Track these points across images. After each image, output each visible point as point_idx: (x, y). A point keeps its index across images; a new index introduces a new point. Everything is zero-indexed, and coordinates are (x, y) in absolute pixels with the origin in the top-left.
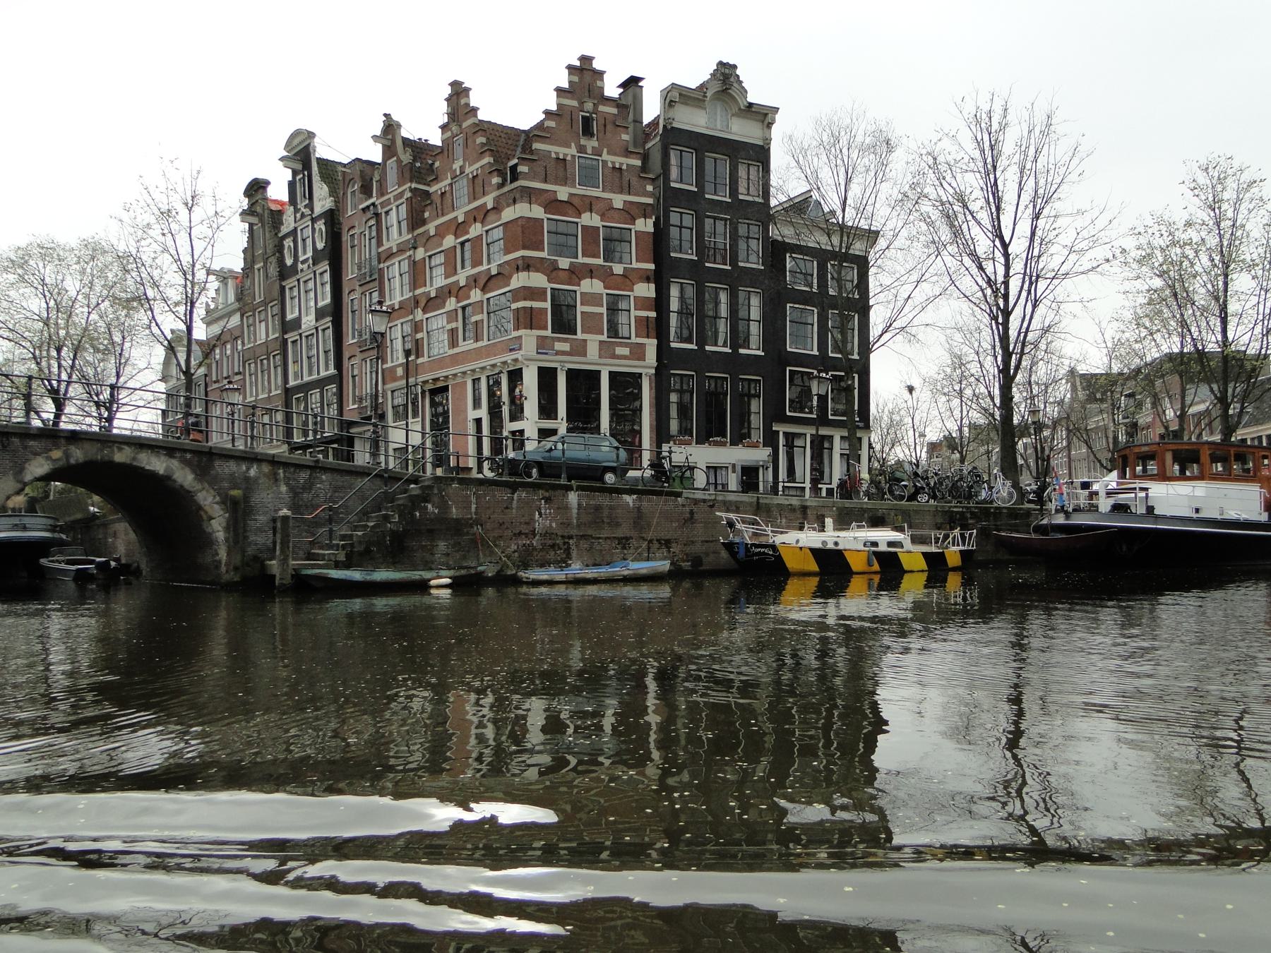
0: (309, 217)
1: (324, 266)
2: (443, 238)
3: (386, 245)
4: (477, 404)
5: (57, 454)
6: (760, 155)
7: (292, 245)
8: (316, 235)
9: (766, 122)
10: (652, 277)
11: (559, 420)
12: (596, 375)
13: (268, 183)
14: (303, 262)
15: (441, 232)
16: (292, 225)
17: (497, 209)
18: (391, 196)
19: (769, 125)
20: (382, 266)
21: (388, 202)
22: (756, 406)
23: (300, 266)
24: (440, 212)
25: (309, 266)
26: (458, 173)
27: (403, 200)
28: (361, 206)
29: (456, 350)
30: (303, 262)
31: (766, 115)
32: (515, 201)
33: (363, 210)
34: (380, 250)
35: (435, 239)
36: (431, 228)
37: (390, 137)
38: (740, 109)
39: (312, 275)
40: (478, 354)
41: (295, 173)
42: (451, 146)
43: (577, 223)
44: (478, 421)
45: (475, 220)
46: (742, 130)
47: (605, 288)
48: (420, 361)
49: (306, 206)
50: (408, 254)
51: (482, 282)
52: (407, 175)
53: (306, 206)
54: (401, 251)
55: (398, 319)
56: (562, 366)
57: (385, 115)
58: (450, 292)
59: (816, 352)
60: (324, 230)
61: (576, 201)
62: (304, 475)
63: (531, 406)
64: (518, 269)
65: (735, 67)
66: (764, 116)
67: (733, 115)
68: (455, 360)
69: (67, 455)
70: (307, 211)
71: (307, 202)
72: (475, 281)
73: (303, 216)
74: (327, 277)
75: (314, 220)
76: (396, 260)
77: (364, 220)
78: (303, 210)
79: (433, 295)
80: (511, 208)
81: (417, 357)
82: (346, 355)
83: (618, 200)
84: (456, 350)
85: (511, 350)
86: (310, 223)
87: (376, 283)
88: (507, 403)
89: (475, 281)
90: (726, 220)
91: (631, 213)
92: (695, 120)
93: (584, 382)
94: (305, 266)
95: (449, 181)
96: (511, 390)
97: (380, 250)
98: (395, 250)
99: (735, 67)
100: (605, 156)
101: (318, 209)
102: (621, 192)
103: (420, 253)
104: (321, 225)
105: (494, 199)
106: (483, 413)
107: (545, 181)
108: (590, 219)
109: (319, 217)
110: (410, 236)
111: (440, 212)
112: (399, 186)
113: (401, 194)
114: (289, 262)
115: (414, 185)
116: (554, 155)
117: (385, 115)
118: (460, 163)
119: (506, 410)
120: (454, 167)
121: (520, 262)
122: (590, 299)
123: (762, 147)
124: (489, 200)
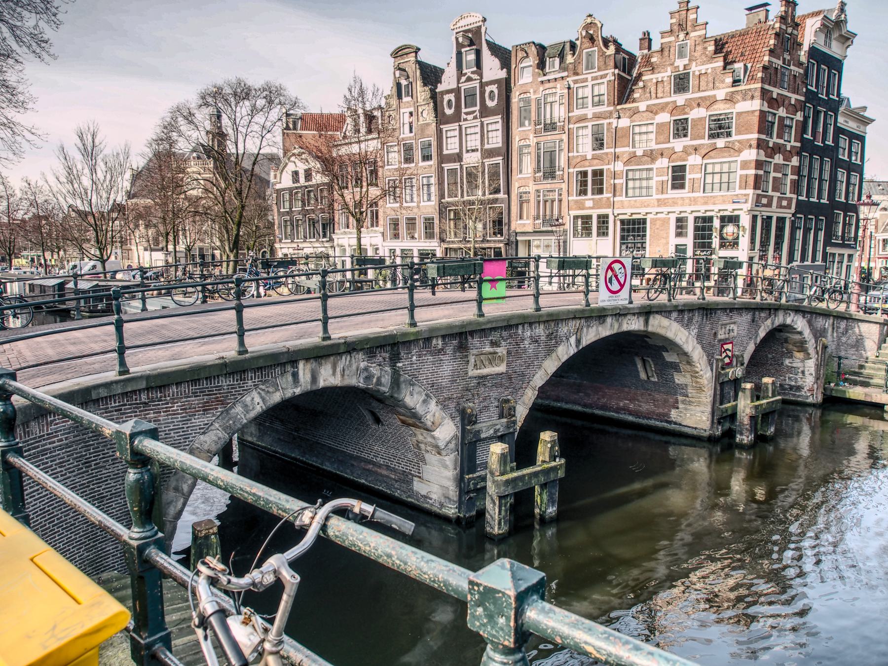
1: (498, 118)
2: (656, 113)
3: (577, 113)
5: (769, 322)
13: (419, 49)
14: (467, 114)
15: (653, 111)
17: (730, 99)
18: (589, 77)
20: (571, 126)
21: (586, 80)
22: (821, 235)
23: (464, 116)
24: (653, 95)
26: (681, 68)
27: (605, 80)
28: (540, 79)
29: (664, 196)
30: (467, 114)
32: (752, 97)
33: (542, 82)
34: (570, 114)
35: (644, 115)
36: (642, 106)
37: (591, 32)
39: (479, 124)
40: (694, 201)
41: (459, 46)
45: (699, 105)
46: (835, 50)
47: (784, 160)
48: (616, 199)
49: (473, 73)
50: (608, 121)
51: (704, 152)
52: (612, 64)
53: (473, 73)
54: (597, 116)
58: (662, 154)
59: (843, 200)
61: (779, 100)
62: (843, 324)
63: (744, 241)
65: (845, 4)
68: (660, 203)
69: (773, 324)
72: (696, 150)
73: (469, 79)
75: (483, 85)
76: (590, 124)
77: (541, 89)
78: (469, 74)
79: (639, 153)
80: (750, 102)
81: (614, 196)
83: (794, 97)
84: (664, 196)
86: (478, 85)
89: (696, 150)
91: (794, 109)
94: (470, 117)
95: (669, 73)
96: (722, 227)
97: (570, 114)
98: (590, 116)
99: (845, 4)
100: (792, 67)
101: (488, 76)
102: (794, 93)
103: (624, 122)
104: (494, 88)
105: (727, 94)
107: (769, 84)
108: (782, 112)
110: (611, 108)
111: (653, 95)
112: (599, 70)
113: (605, 76)
114: (449, 112)
115: (617, 71)
118: (686, 61)
119: (716, 242)
120: (676, 64)
121: (754, 143)
122: (777, 168)
124: (721, 94)
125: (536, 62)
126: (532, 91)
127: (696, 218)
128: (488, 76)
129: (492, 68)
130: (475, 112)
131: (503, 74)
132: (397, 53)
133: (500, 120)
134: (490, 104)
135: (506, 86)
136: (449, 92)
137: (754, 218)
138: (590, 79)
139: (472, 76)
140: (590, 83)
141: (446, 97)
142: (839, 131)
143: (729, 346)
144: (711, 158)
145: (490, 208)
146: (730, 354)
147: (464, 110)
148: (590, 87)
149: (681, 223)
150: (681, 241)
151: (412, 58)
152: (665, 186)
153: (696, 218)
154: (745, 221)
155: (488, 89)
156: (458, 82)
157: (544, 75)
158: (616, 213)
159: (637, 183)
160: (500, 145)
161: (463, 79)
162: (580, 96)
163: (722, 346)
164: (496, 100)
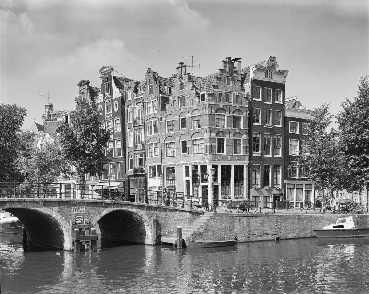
0: (111, 99)
1: (119, 118)
4: (187, 175)
6: (282, 87)
7: (102, 108)
8: (114, 106)
9: (284, 75)
10: (248, 132)
11: (219, 182)
12: (230, 166)
14: (108, 115)
16: (102, 101)
19: (285, 77)
23: (106, 116)
25: (110, 117)
28: (135, 98)
30: (108, 115)
31: (284, 73)
38: (276, 72)
42: (178, 85)
43: (225, 115)
44: (188, 181)
46: (276, 79)
49: (109, 95)
53: (109, 95)
55: (153, 141)
56: (220, 164)
57: (149, 69)
60: (118, 104)
61: (225, 108)
63: (210, 179)
64: (207, 132)
65: (275, 58)
66: (283, 73)
67: (273, 74)
70: (110, 97)
71: (109, 93)
74: (119, 122)
76: (152, 121)
77: (136, 103)
78: (107, 95)
82: (127, 151)
85: (203, 159)
87: (143, 127)
88: (200, 175)
90: (270, 111)
92: (261, 77)
93: (226, 169)
94: (109, 117)
99: (275, 58)
101: (115, 96)
104: (116, 102)
106: (190, 178)
109: (115, 100)
116: (218, 92)
117: (149, 69)
119: (200, 178)
121: (208, 130)
123: (282, 84)
125: (133, 90)
126: (132, 104)
127: (201, 166)
128: (115, 96)
129: (116, 92)
130: (110, 114)
131: (120, 95)
132: (81, 84)
133: (119, 118)
134: (116, 110)
135: (122, 100)
136: (99, 104)
137: (216, 166)
138: (151, 99)
139: (108, 96)
140: (151, 101)
141: (99, 107)
142: (286, 119)
143: (82, 217)
144: (150, 142)
145: (111, 164)
146: (82, 219)
147: (106, 113)
148: (151, 102)
149: (187, 168)
150: (188, 178)
151: (86, 87)
152: (179, 152)
153: (201, 166)
154: (210, 168)
155: (115, 103)
156: (104, 100)
157: (137, 96)
158: (163, 164)
159: (170, 150)
160: (120, 131)
161: (105, 98)
162: (148, 107)
163: (76, 216)
164: (118, 109)
